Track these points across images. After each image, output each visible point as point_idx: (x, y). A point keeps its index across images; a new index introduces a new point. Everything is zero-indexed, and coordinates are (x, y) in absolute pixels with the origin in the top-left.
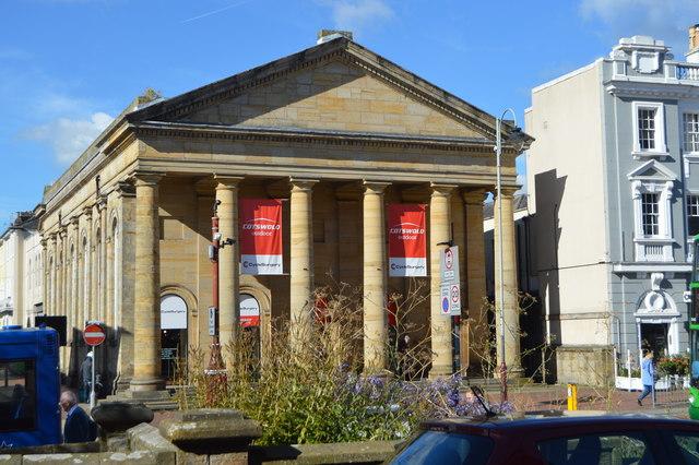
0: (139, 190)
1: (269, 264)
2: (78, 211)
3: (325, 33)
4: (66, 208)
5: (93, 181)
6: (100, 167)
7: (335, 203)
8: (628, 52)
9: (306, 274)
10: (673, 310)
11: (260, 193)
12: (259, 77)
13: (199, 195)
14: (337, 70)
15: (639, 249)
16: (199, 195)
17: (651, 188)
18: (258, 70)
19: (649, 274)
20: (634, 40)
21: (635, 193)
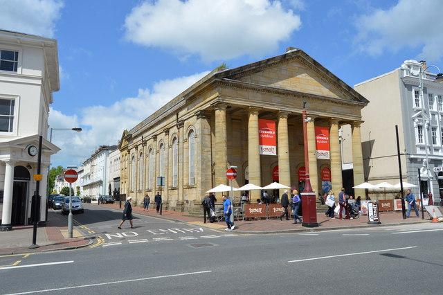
0: (217, 112)
1: (269, 151)
2: (157, 133)
3: (291, 48)
4: (145, 135)
5: (175, 117)
6: (181, 109)
7: (296, 124)
8: (409, 66)
9: (288, 155)
10: (431, 175)
11: (268, 117)
12: (269, 63)
13: (232, 119)
14: (295, 65)
15: (418, 149)
16: (232, 119)
17: (421, 124)
18: (268, 60)
19: (422, 159)
20: (411, 61)
21: (415, 125)
